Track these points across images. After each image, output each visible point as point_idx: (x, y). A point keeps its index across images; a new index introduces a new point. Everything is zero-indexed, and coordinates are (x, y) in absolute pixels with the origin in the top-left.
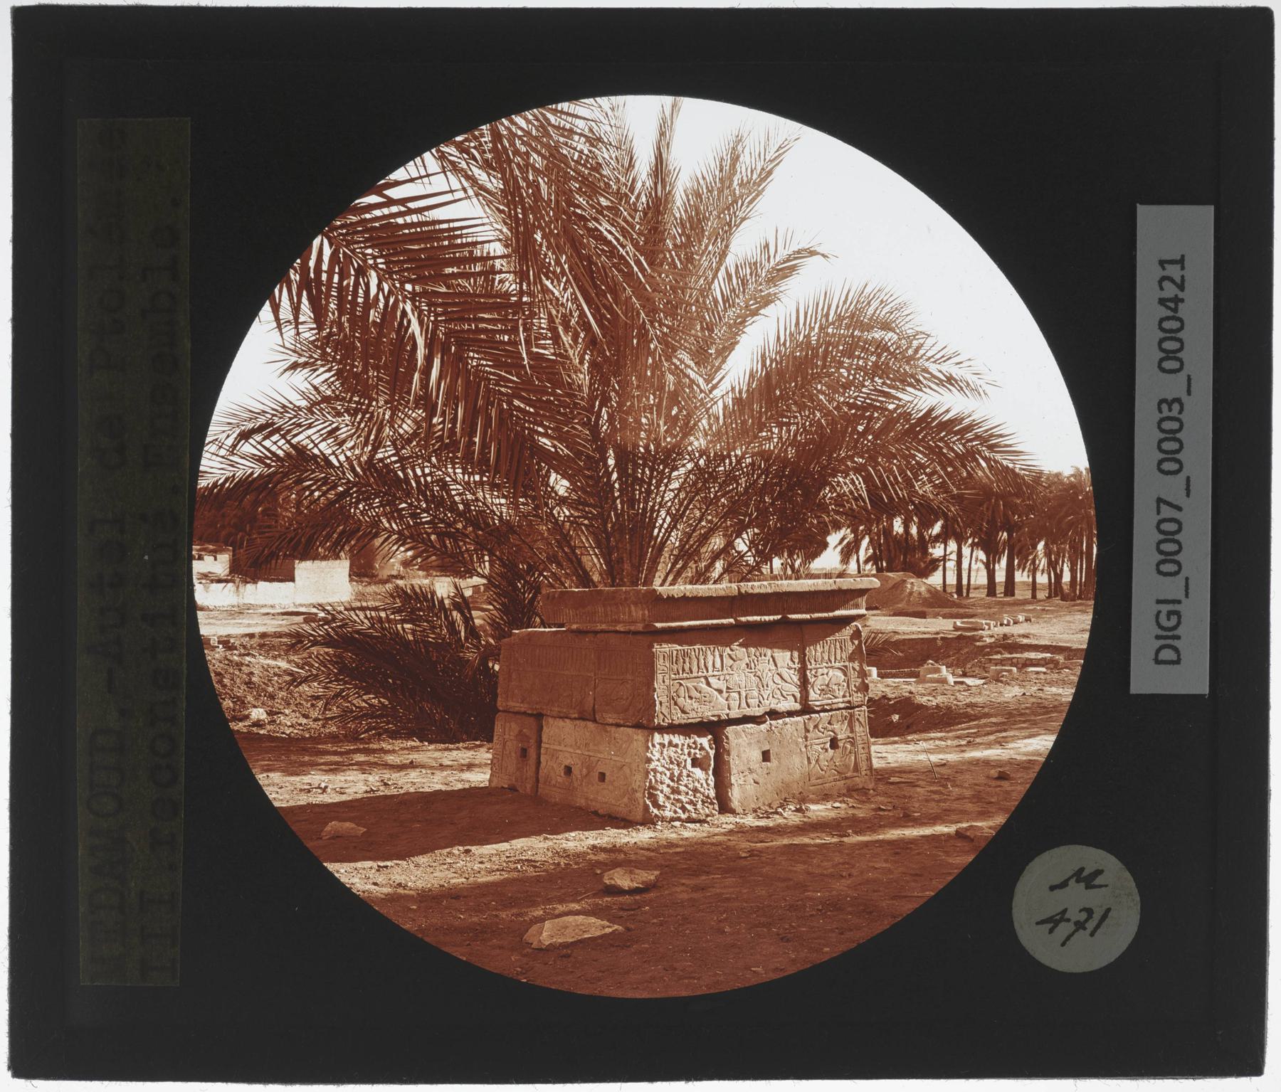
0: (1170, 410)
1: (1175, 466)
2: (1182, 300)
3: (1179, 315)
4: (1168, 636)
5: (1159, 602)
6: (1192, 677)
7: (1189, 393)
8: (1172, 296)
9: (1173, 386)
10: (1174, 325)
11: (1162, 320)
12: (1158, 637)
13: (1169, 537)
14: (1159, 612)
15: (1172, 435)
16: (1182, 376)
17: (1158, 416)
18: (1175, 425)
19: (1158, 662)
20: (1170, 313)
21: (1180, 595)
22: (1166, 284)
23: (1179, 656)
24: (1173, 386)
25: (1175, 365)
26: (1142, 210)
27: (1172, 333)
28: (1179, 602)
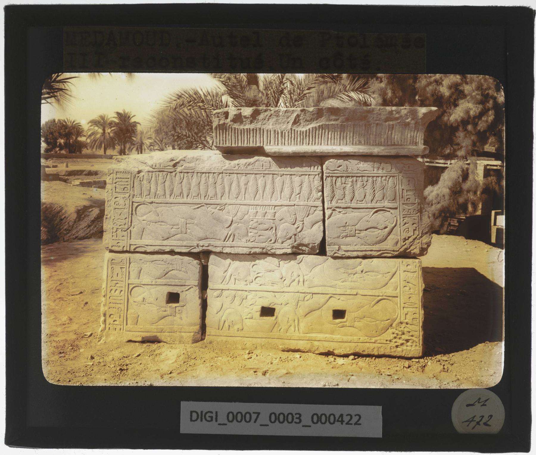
0: (297, 418)
2: (342, 424)
3: (336, 422)
4: (202, 416)
5: (216, 413)
6: (187, 427)
7: (303, 426)
9: (306, 420)
10: (332, 420)
12: (202, 412)
14: (212, 412)
15: (286, 418)
16: (310, 423)
17: (294, 415)
18: (290, 420)
20: (337, 419)
22: (349, 417)
23: (194, 421)
24: (306, 420)
26: (380, 408)
27: (328, 419)
28: (216, 421)
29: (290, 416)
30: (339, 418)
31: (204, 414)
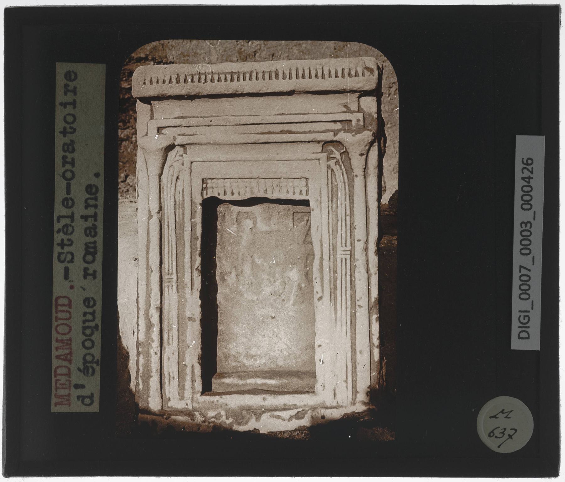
2: (532, 178)
4: (524, 326)
5: (520, 311)
6: (534, 344)
7: (534, 219)
8: (527, 176)
9: (527, 216)
11: (523, 187)
12: (520, 327)
13: (525, 283)
14: (520, 316)
15: (526, 238)
16: (531, 212)
18: (528, 233)
19: (519, 338)
20: (526, 184)
22: (525, 171)
23: (529, 336)
24: (527, 216)
25: (529, 207)
28: (529, 312)
29: (524, 233)
30: (526, 181)
31: (522, 325)
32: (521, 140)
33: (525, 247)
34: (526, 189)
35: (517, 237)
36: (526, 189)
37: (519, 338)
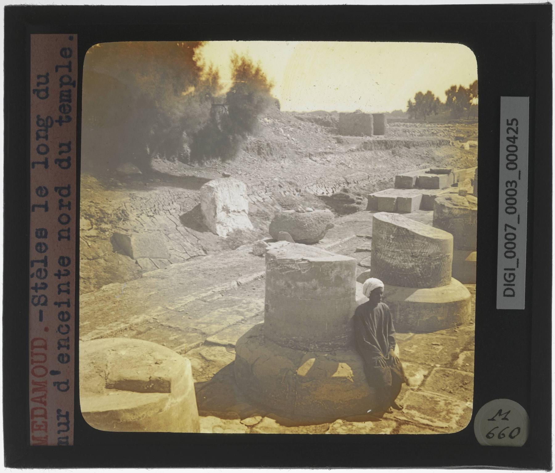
0: (511, 186)
1: (513, 210)
2: (517, 138)
4: (509, 284)
5: (505, 269)
7: (520, 179)
9: (512, 175)
10: (513, 149)
11: (508, 147)
12: (505, 285)
13: (510, 241)
14: (505, 274)
15: (511, 197)
16: (517, 171)
17: (507, 188)
18: (513, 193)
19: (505, 295)
20: (511, 144)
21: (514, 266)
22: (510, 131)
24: (512, 175)
28: (514, 269)
29: (509, 192)
30: (510, 141)
32: (505, 101)
33: (511, 206)
34: (511, 149)
35: (502, 197)
36: (511, 149)
37: (505, 295)
